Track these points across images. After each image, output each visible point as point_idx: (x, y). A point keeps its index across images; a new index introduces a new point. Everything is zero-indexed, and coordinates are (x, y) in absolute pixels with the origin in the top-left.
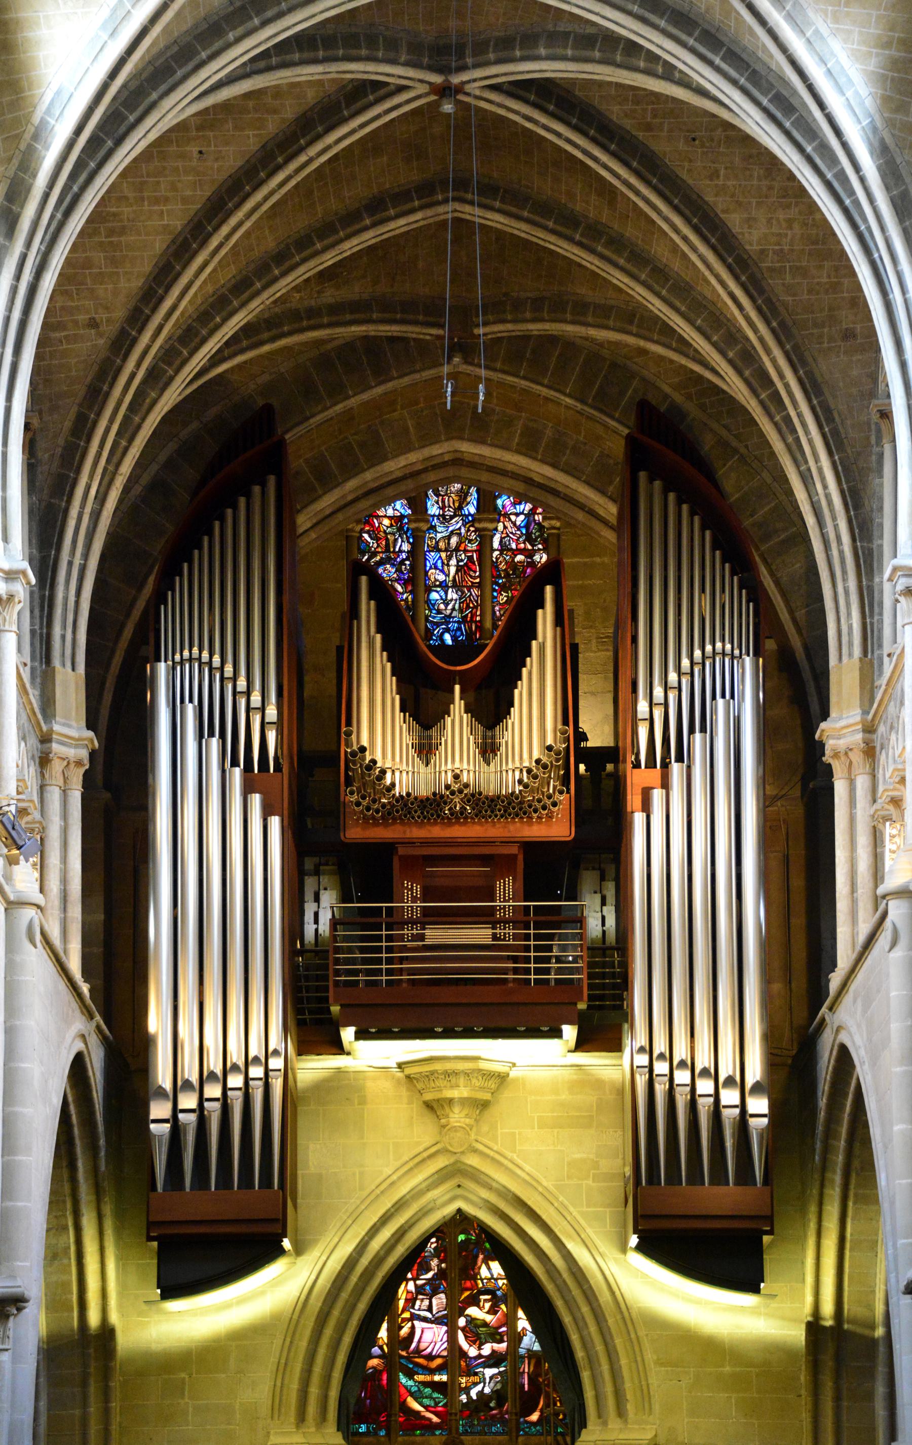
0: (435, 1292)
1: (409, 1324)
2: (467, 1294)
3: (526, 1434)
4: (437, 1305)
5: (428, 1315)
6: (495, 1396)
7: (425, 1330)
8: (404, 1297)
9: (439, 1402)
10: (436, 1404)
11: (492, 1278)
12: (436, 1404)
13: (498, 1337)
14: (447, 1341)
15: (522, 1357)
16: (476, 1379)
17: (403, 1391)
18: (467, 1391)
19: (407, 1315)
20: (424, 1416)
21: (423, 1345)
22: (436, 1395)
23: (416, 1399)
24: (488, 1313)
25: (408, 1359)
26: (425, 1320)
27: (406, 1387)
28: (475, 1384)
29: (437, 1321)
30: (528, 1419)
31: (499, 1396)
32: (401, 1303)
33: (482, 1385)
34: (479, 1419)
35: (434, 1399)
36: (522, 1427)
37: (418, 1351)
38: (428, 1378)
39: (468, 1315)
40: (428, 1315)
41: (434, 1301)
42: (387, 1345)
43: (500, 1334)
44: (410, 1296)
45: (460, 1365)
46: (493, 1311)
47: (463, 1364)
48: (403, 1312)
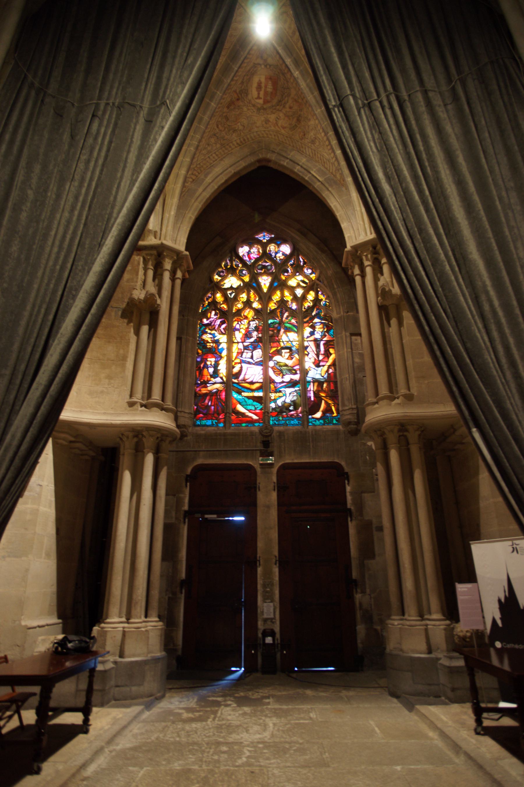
0: (255, 348)
1: (239, 365)
2: (274, 349)
3: (314, 425)
5: (251, 360)
6: (292, 404)
7: (249, 369)
9: (257, 408)
10: (256, 409)
11: (290, 341)
12: (256, 409)
13: (294, 372)
15: (310, 382)
16: (281, 394)
17: (235, 401)
18: (275, 401)
19: (238, 361)
22: (255, 403)
23: (242, 406)
24: (287, 359)
26: (249, 363)
29: (257, 364)
31: (294, 404)
33: (285, 397)
34: (283, 417)
35: (254, 406)
36: (310, 420)
37: (244, 380)
38: (250, 394)
39: (275, 360)
40: (251, 360)
42: (226, 377)
43: (294, 370)
44: (240, 351)
46: (291, 357)
47: (272, 386)
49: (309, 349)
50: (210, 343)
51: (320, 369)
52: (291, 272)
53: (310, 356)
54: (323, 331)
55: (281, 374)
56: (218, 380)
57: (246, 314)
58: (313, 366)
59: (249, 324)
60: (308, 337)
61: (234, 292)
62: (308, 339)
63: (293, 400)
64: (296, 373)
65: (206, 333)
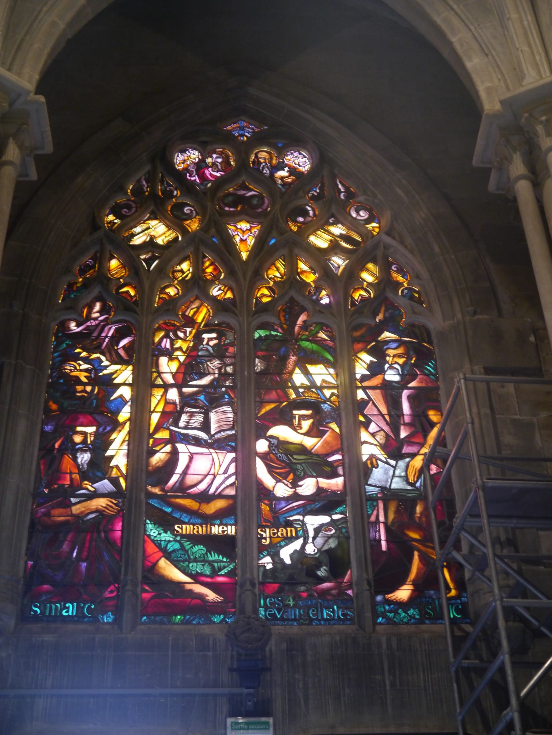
1: (168, 448)
2: (269, 407)
3: (389, 621)
4: (219, 421)
5: (202, 435)
6: (325, 559)
7: (195, 457)
8: (160, 408)
9: (220, 569)
10: (215, 572)
11: (313, 385)
12: (215, 572)
13: (328, 469)
14: (236, 473)
15: (373, 499)
17: (151, 549)
19: (164, 434)
20: (191, 591)
21: (190, 480)
22: (214, 557)
23: (176, 563)
24: (307, 434)
25: (164, 499)
26: (198, 442)
27: (158, 544)
28: (289, 540)
30: (390, 596)
32: (155, 418)
33: (300, 541)
35: (211, 563)
36: (380, 609)
39: (272, 437)
40: (202, 435)
41: (213, 417)
42: (126, 478)
43: (330, 464)
44: (169, 408)
45: (259, 510)
47: (265, 508)
48: (157, 430)
49: (369, 410)
50: (85, 384)
51: (402, 464)
52: (315, 215)
53: (373, 428)
54: (405, 363)
55: (291, 476)
56: (105, 485)
57: (190, 313)
58: (381, 454)
59: (198, 338)
60: (364, 378)
61: (156, 258)
62: (366, 384)
63: (326, 548)
64: (336, 475)
65: (77, 357)
